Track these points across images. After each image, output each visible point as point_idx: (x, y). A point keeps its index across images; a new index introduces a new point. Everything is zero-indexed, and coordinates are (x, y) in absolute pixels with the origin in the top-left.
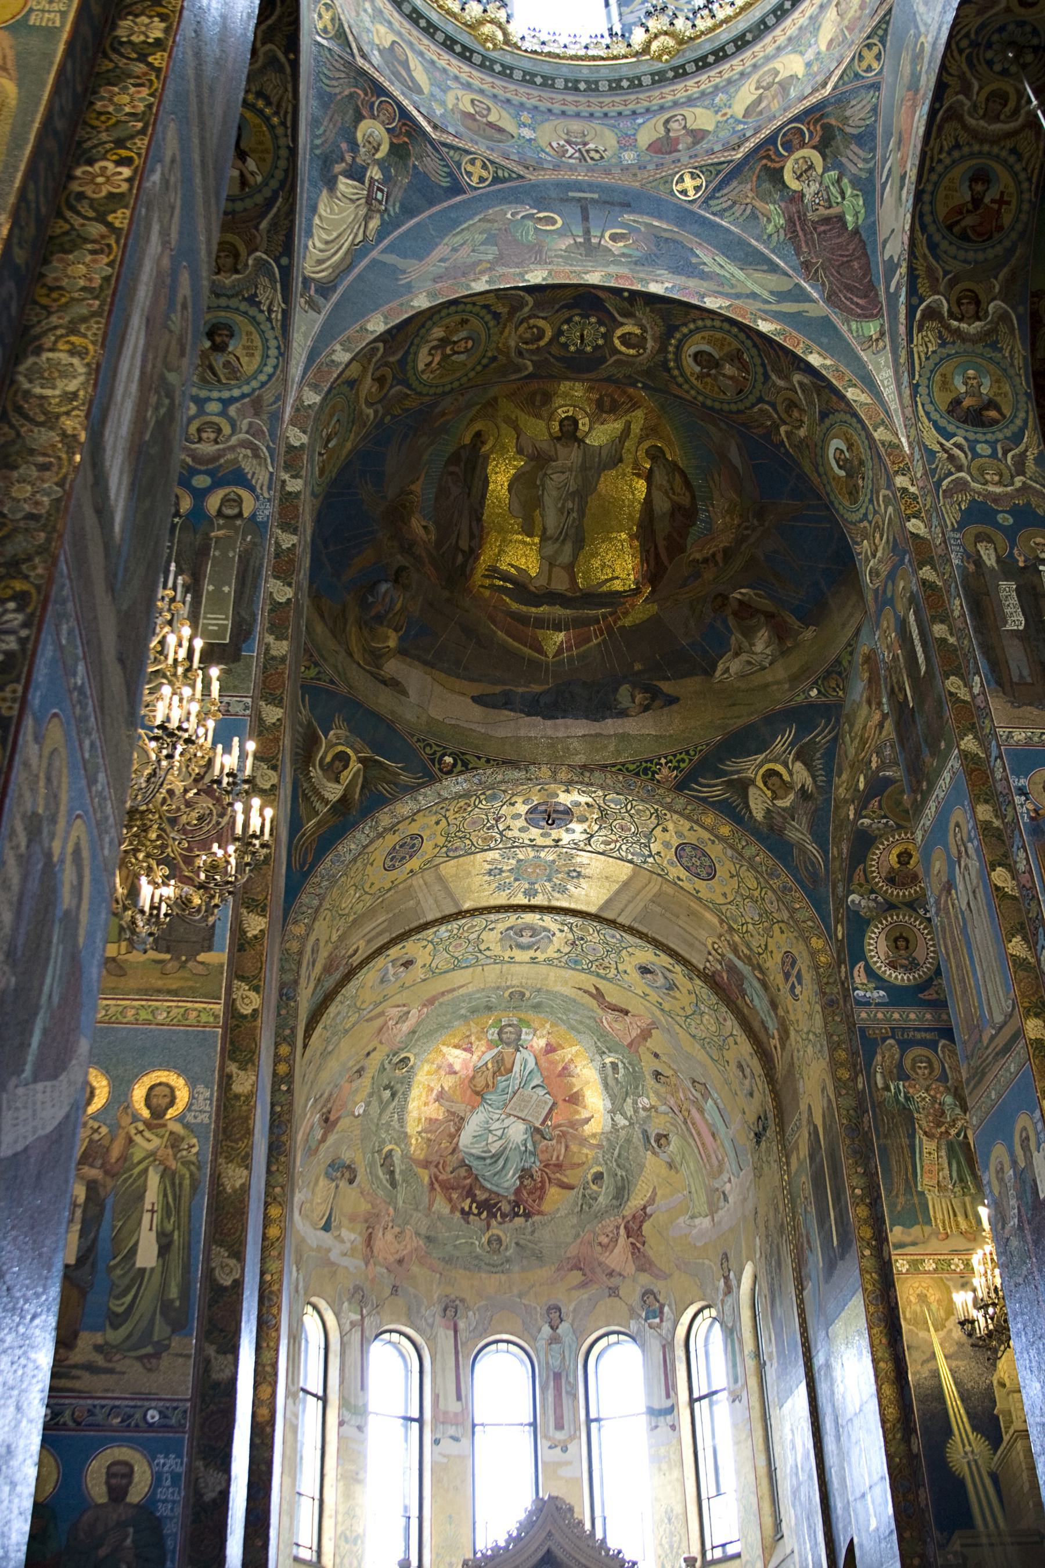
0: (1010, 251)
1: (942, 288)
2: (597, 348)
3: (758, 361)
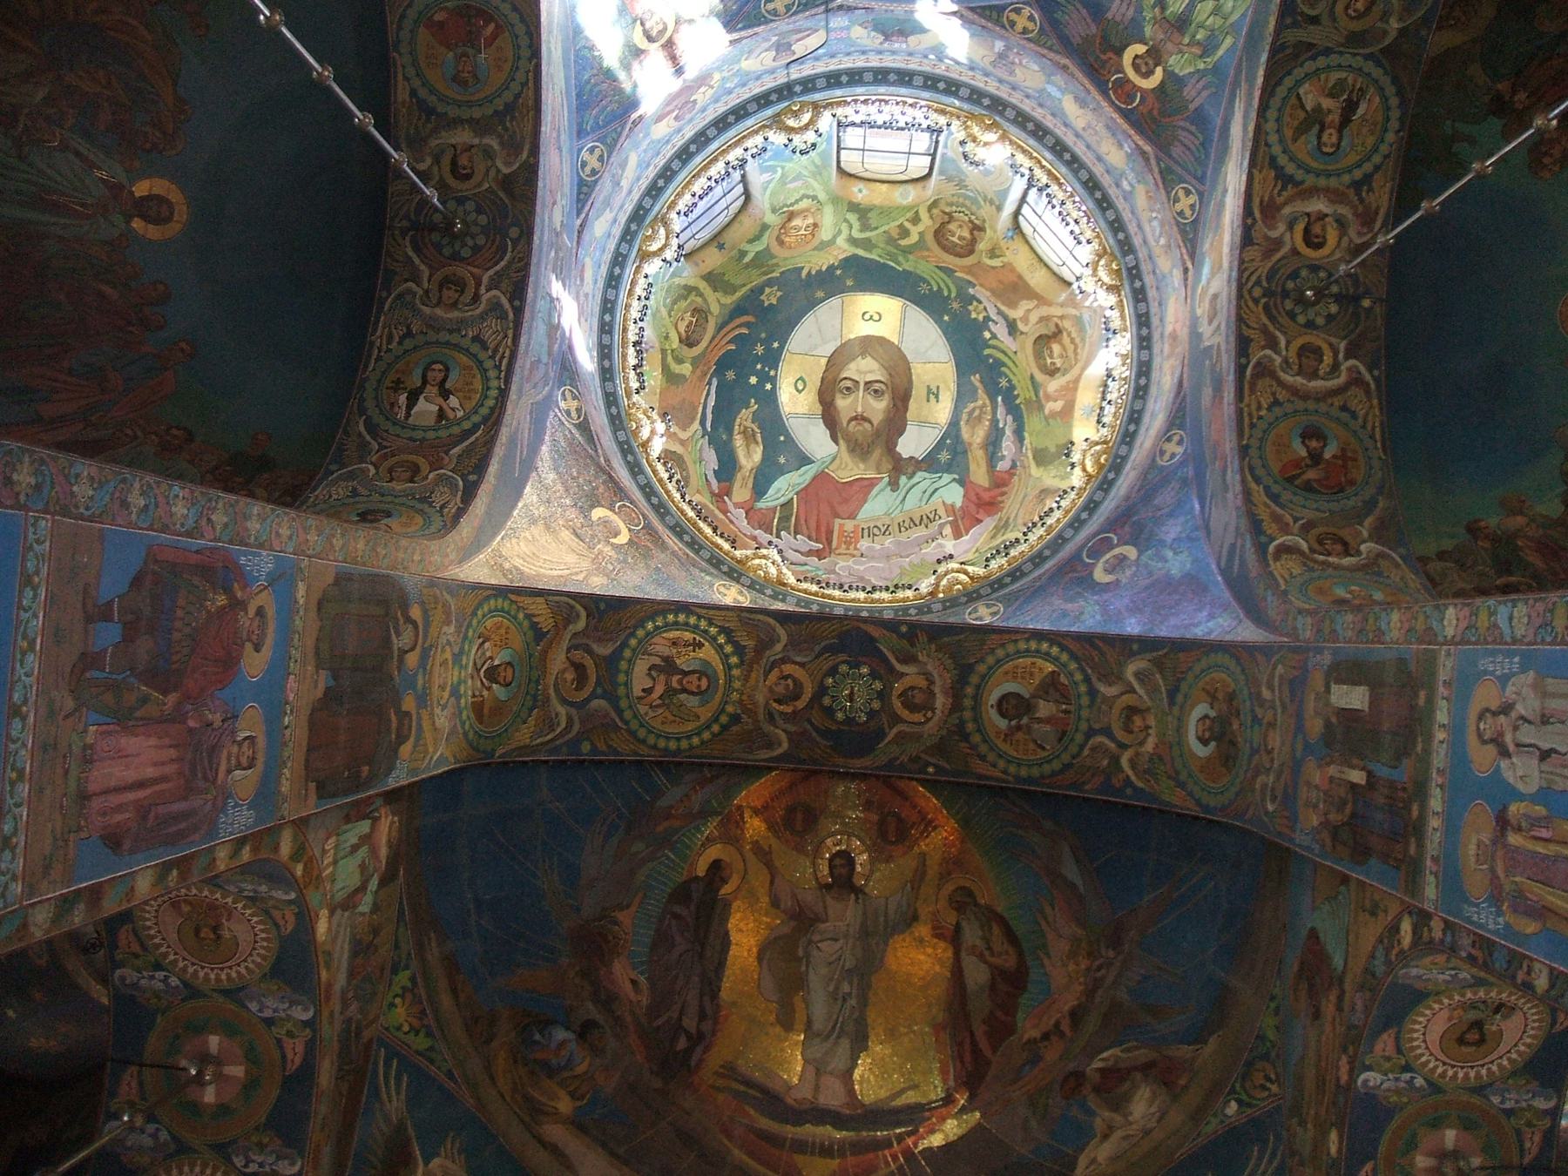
0: (1370, 505)
1: (1296, 531)
2: (872, 714)
3: (1078, 677)
